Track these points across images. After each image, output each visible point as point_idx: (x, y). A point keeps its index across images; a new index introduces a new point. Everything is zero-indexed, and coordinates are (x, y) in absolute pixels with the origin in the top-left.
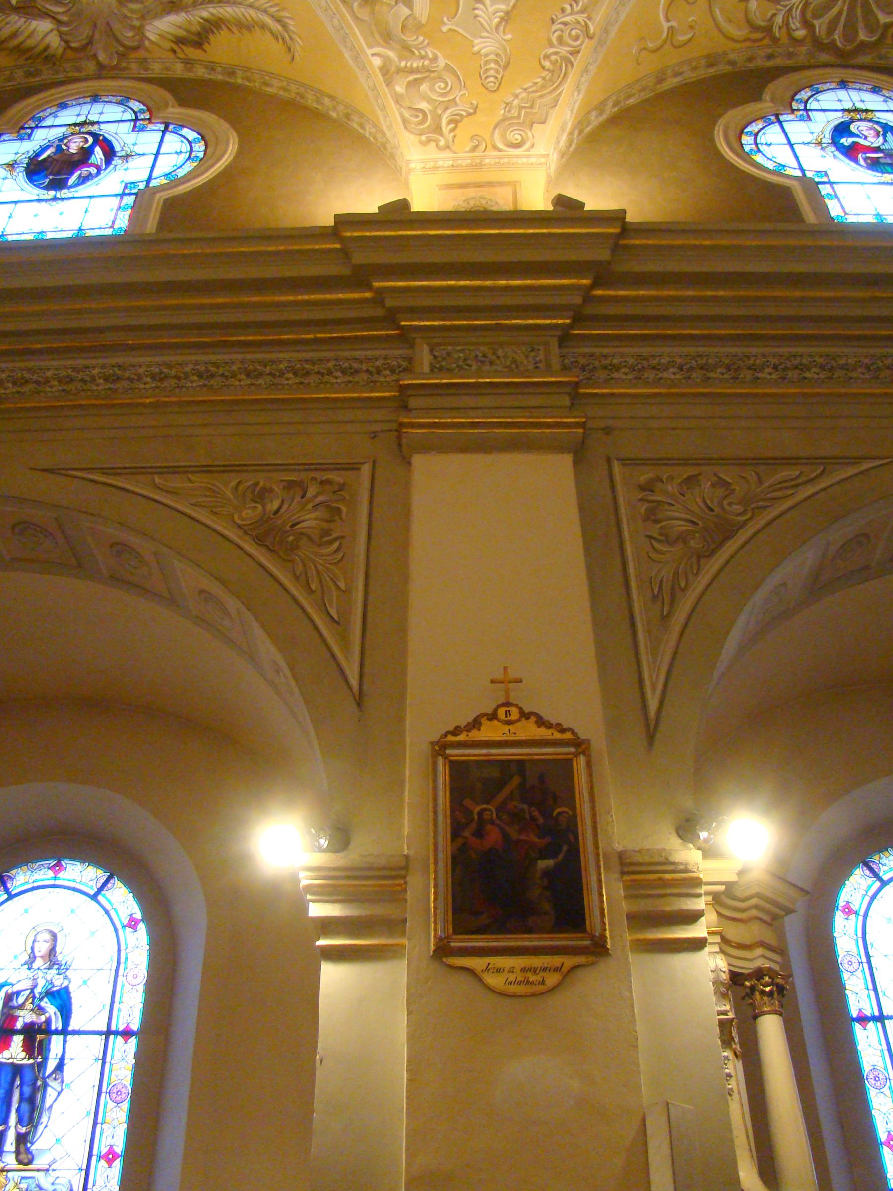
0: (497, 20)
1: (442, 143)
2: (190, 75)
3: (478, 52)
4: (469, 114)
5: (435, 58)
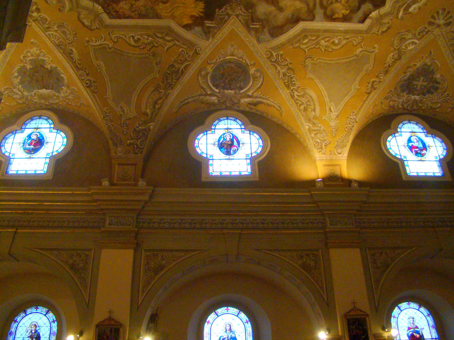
0: (335, 117)
1: (323, 152)
2: (251, 111)
3: (331, 126)
4: (329, 144)
5: (320, 127)
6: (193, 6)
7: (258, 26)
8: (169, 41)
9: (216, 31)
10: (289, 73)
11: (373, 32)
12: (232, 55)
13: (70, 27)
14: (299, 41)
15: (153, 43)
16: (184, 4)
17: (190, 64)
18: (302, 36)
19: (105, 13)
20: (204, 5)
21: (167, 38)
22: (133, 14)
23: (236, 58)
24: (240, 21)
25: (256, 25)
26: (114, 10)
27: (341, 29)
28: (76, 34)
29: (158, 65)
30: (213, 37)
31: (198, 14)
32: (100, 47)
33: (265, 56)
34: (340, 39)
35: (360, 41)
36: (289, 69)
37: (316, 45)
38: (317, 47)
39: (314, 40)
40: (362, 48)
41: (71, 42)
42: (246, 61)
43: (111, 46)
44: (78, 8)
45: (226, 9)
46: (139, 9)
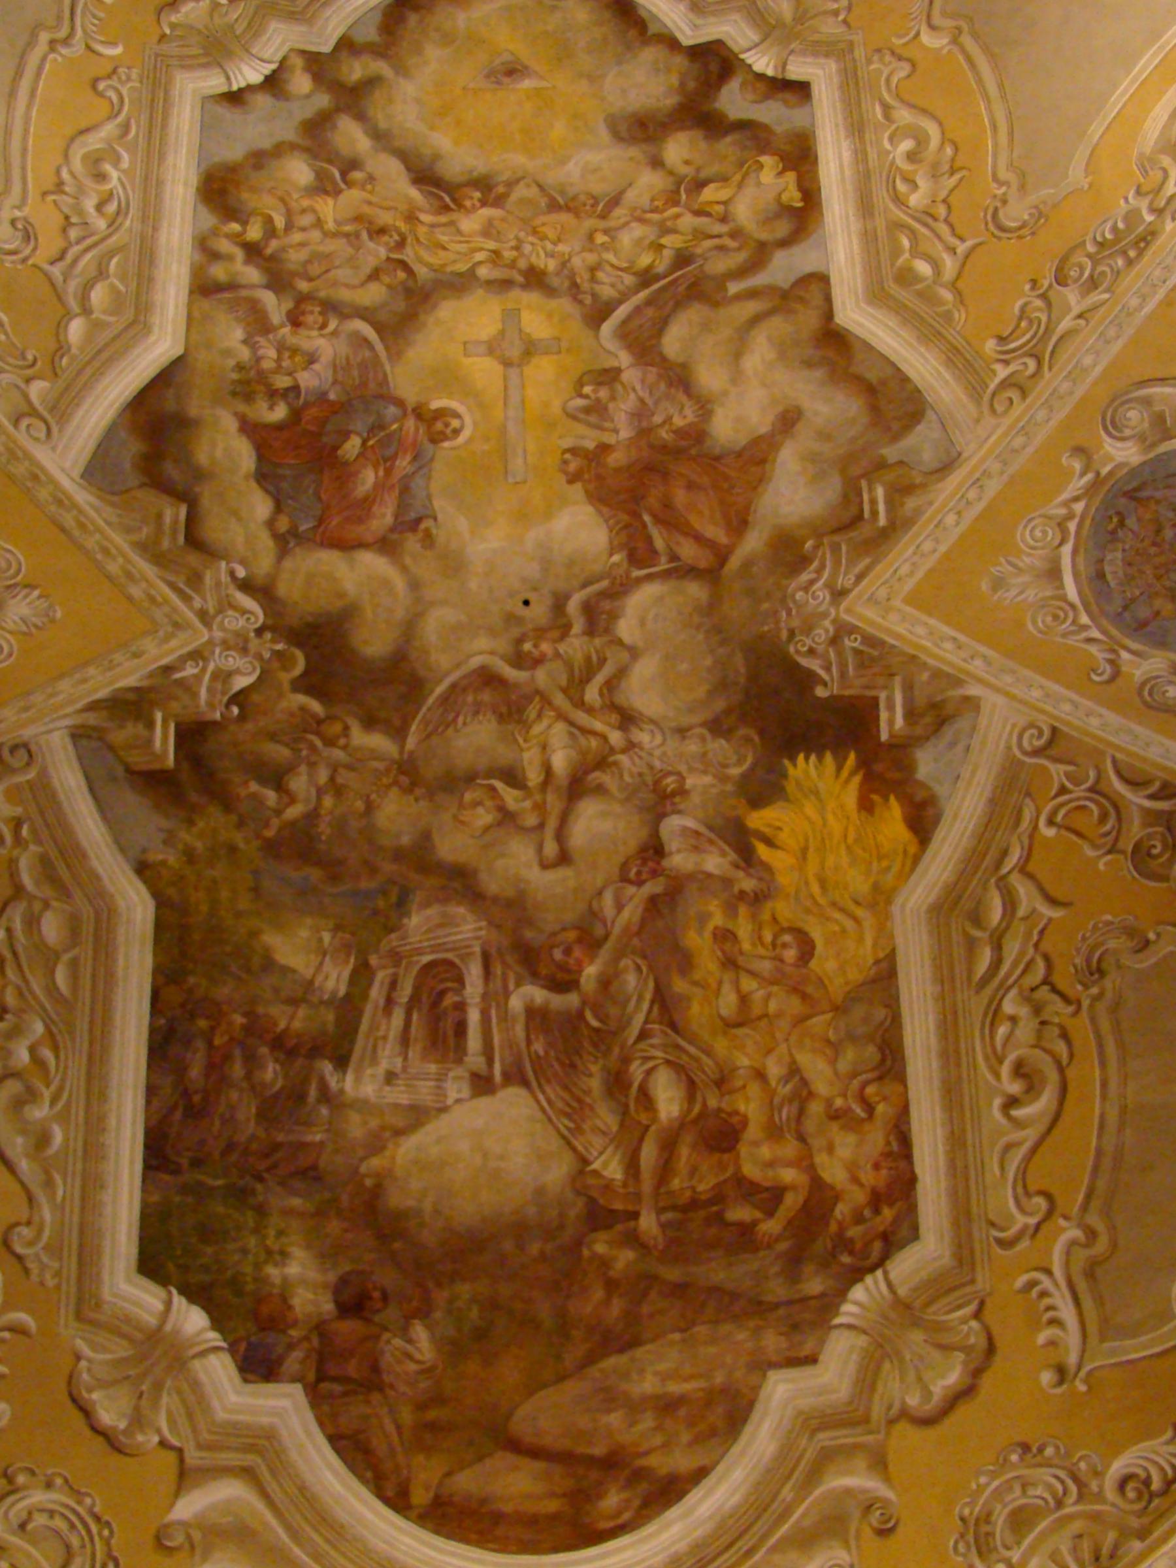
6: (810, 809)
7: (880, 492)
8: (1010, 905)
9: (925, 676)
10: (1082, 269)
11: (842, 29)
12: (1053, 573)
13: (983, 1480)
14: (927, 296)
15: (1033, 990)
16: (804, 851)
17: (1115, 762)
18: (903, 295)
19: (889, 1265)
20: (801, 757)
21: (995, 914)
22: (880, 1108)
23: (1067, 549)
24: (860, 577)
25: (873, 502)
26: (867, 1213)
27: (847, 155)
28: (1025, 1448)
29: (1147, 943)
30: (958, 683)
31: (847, 781)
32: (1088, 1303)
33: (1018, 408)
34: (891, 139)
35: (888, 58)
36: (1061, 279)
37: (935, 219)
38: (942, 211)
39: (914, 236)
40: (918, 34)
41: (1076, 1479)
42: (1076, 499)
43: (1075, 1233)
44: (866, 1420)
45: (811, 652)
46: (854, 1075)
